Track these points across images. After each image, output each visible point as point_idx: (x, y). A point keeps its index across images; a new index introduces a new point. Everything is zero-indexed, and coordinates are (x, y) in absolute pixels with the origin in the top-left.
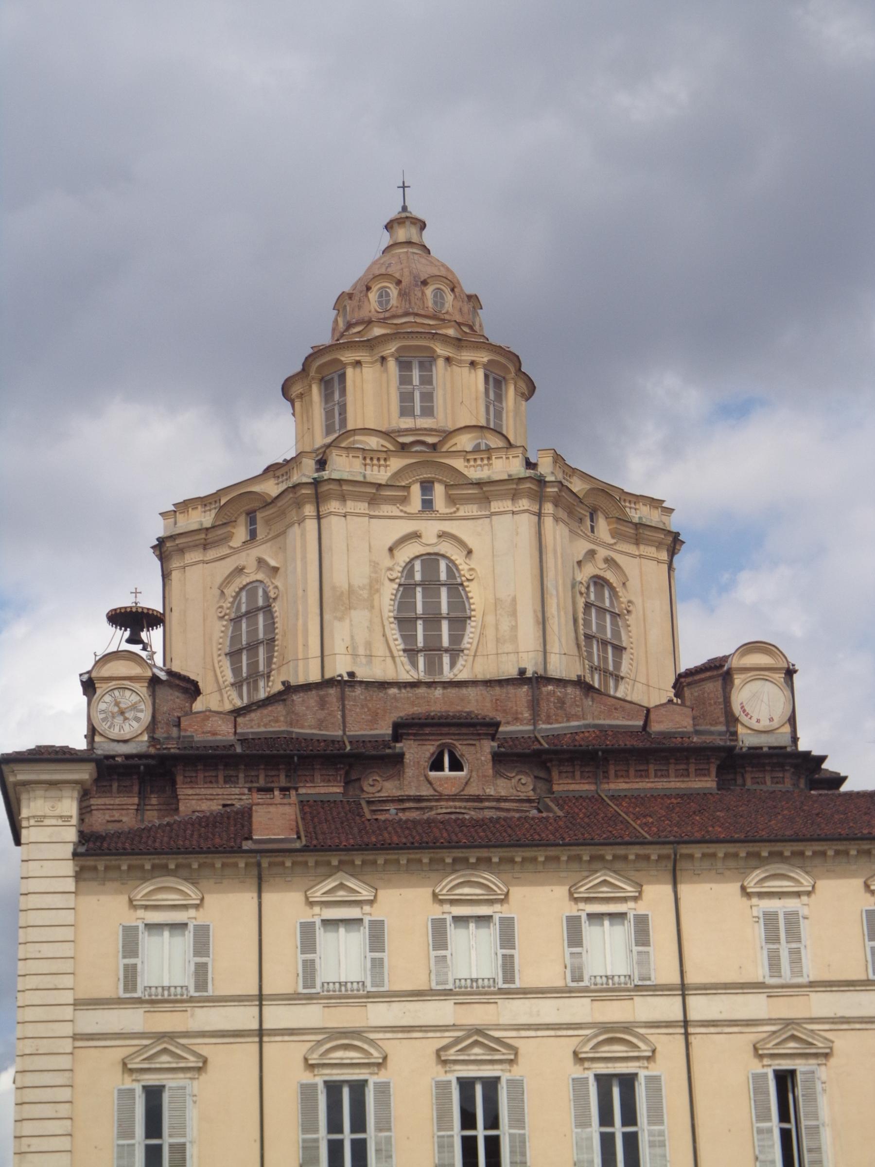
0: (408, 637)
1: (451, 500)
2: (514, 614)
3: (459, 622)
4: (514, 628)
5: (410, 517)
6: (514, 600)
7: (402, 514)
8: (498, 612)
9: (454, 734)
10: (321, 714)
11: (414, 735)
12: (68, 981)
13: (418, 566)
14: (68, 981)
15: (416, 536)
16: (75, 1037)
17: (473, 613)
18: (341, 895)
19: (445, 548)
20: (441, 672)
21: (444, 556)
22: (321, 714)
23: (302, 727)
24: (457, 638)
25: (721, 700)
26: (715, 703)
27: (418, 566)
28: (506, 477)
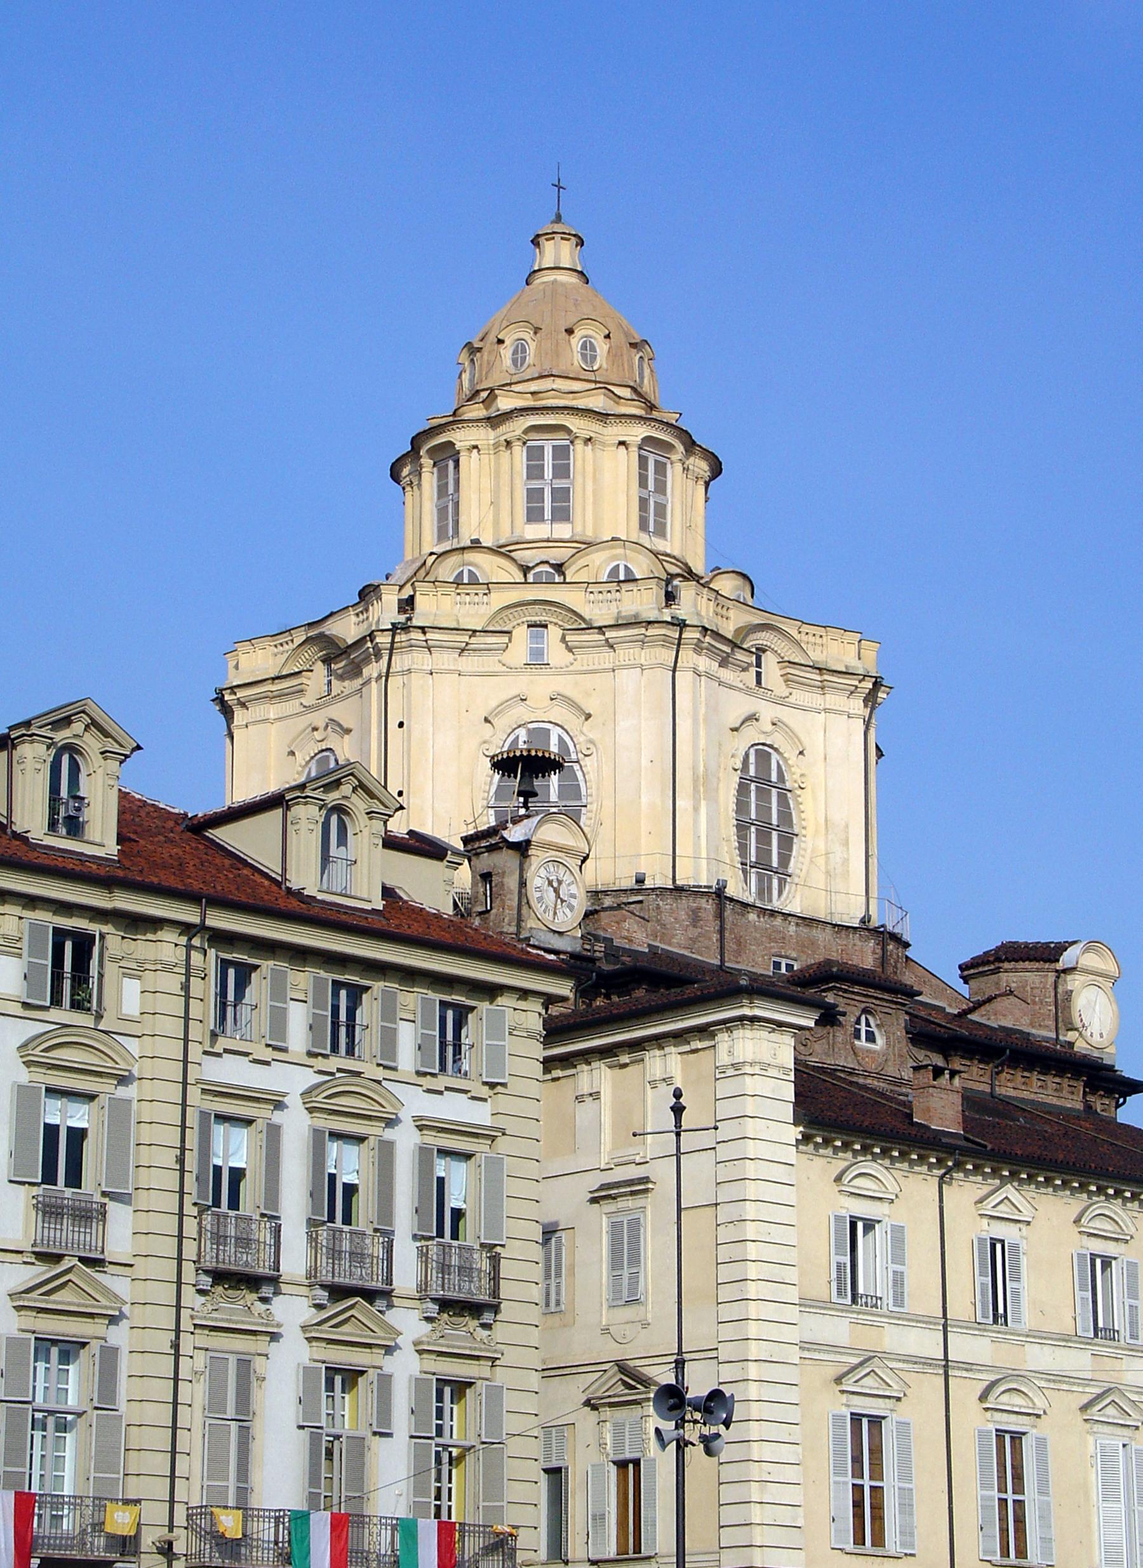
0: (743, 848)
1: (787, 679)
2: (846, 843)
3: (787, 842)
4: (846, 861)
5: (747, 691)
6: (847, 826)
7: (741, 685)
8: (830, 837)
9: (876, 998)
10: (693, 932)
11: (845, 991)
12: (791, 1275)
13: (752, 759)
14: (791, 1275)
15: (752, 718)
16: (805, 1345)
17: (804, 832)
18: (1004, 1211)
19: (777, 739)
20: (770, 901)
21: (776, 750)
22: (693, 932)
23: (670, 944)
24: (785, 859)
25: (1051, 1000)
26: (1041, 1002)
27: (752, 759)
28: (844, 670)
